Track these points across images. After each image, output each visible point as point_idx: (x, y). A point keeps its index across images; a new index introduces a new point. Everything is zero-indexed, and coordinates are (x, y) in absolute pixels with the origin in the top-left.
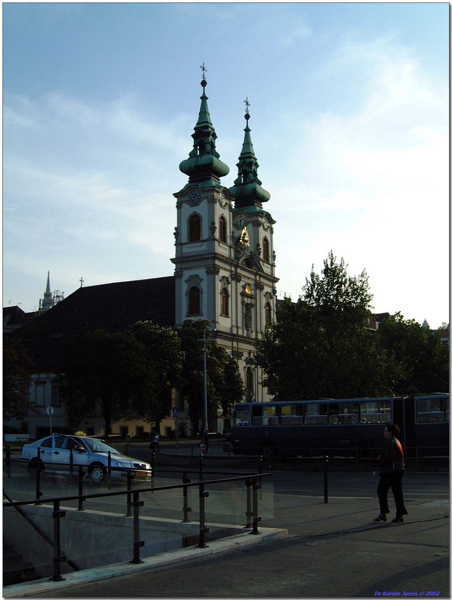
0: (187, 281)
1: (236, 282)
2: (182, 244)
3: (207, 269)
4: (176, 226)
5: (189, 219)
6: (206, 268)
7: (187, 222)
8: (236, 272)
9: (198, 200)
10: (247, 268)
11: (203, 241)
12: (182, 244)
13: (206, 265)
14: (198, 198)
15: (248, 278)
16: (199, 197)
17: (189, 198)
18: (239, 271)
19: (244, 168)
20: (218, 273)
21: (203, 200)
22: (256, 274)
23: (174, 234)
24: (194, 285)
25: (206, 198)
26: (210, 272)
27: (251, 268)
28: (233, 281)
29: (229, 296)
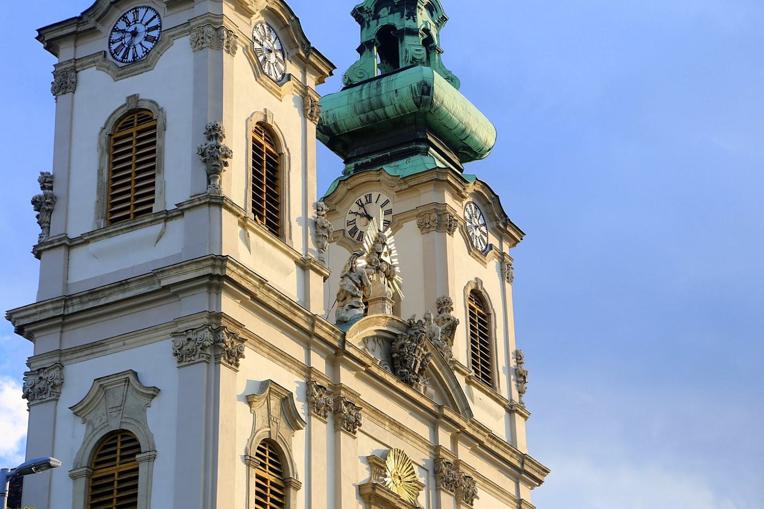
0: (78, 410)
1: (336, 429)
2: (70, 244)
3: (182, 340)
4: (49, 169)
5: (109, 130)
6: (175, 335)
7: (101, 147)
8: (337, 387)
9: (149, 45)
10: (392, 381)
11: (168, 216)
12: (70, 244)
13: (177, 322)
14: (146, 39)
15: (399, 428)
16: (155, 33)
17: (111, 42)
18: (347, 378)
19: (383, 22)
20: (234, 358)
21: (169, 44)
22: (435, 419)
23: (37, 203)
24: (115, 426)
25: (186, 27)
26: (191, 353)
27: (408, 383)
28: (314, 420)
29: (297, 488)
